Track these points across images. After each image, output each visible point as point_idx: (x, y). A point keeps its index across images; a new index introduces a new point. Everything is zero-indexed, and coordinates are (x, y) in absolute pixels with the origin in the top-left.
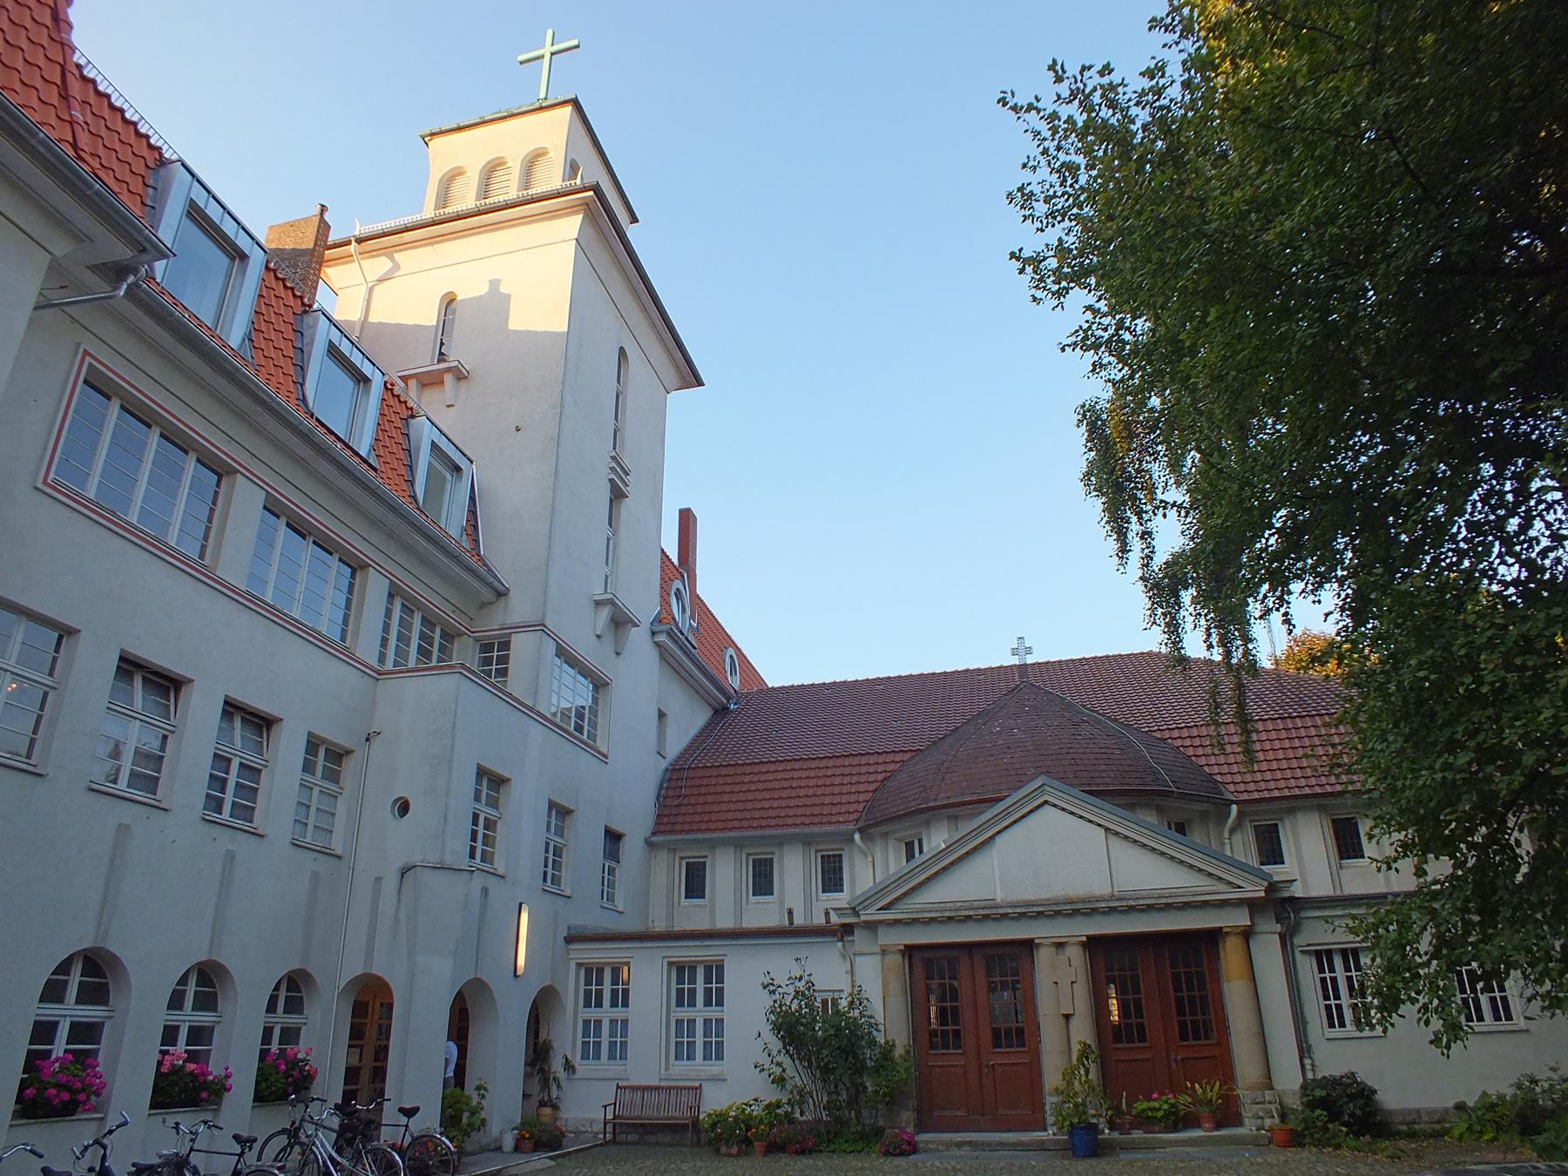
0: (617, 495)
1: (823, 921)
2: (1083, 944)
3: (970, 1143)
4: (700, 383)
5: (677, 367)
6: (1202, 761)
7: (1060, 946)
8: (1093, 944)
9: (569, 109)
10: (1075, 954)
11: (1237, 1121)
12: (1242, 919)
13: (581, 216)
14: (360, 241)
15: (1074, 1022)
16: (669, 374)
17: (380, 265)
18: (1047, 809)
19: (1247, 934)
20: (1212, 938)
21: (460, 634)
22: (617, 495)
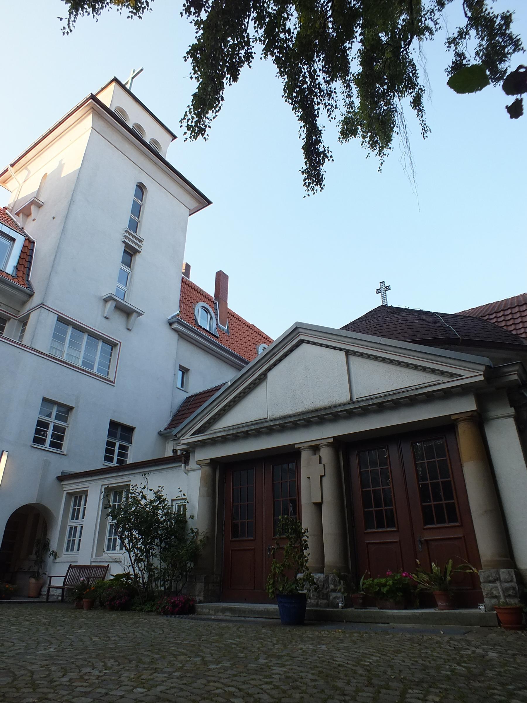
0: (130, 253)
1: (171, 454)
2: (330, 445)
3: (231, 610)
4: (209, 203)
5: (190, 193)
6: (510, 329)
7: (315, 448)
8: (342, 446)
9: (114, 84)
10: (326, 453)
11: (474, 600)
12: (468, 405)
13: (91, 115)
14: (12, 165)
15: (325, 509)
16: (193, 204)
17: (24, 173)
18: (304, 346)
19: (479, 421)
20: (446, 427)
21: (9, 319)
22: (130, 253)
